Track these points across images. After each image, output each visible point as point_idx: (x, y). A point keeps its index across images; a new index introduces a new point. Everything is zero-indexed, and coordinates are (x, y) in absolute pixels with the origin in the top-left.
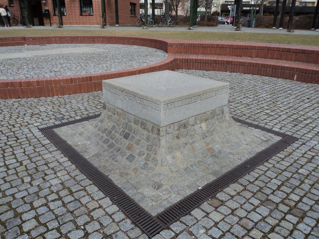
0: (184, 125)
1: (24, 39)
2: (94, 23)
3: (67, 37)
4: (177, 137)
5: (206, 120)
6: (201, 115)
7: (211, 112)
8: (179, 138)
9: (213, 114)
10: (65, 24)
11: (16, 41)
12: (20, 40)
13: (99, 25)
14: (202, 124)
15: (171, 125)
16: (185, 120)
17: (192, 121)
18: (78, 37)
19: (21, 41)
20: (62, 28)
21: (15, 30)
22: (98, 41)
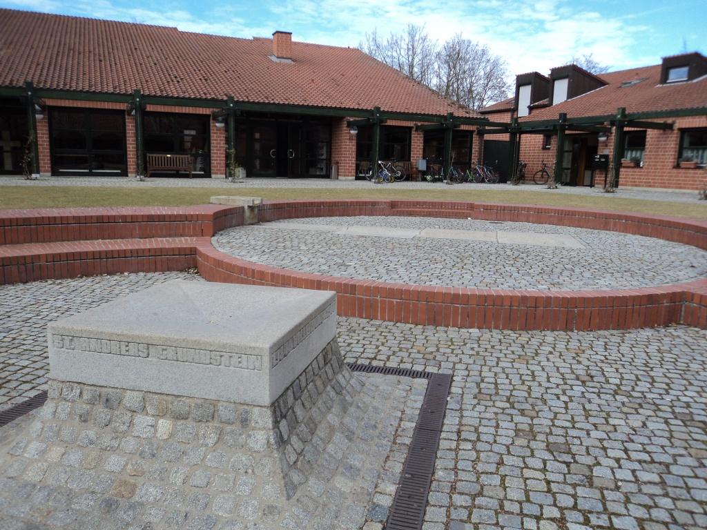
0: (107, 400)
1: (472, 207)
2: (656, 183)
3: (552, 210)
4: (81, 416)
5: (179, 417)
6: (165, 397)
7: (199, 402)
8: (85, 421)
9: (208, 412)
10: (622, 185)
11: (457, 209)
12: (464, 209)
13: (697, 192)
14: (161, 421)
15: (76, 385)
16: (114, 390)
17: (131, 399)
18: (574, 213)
19: (466, 211)
20: (613, 192)
21: (523, 192)
22: (615, 225)
